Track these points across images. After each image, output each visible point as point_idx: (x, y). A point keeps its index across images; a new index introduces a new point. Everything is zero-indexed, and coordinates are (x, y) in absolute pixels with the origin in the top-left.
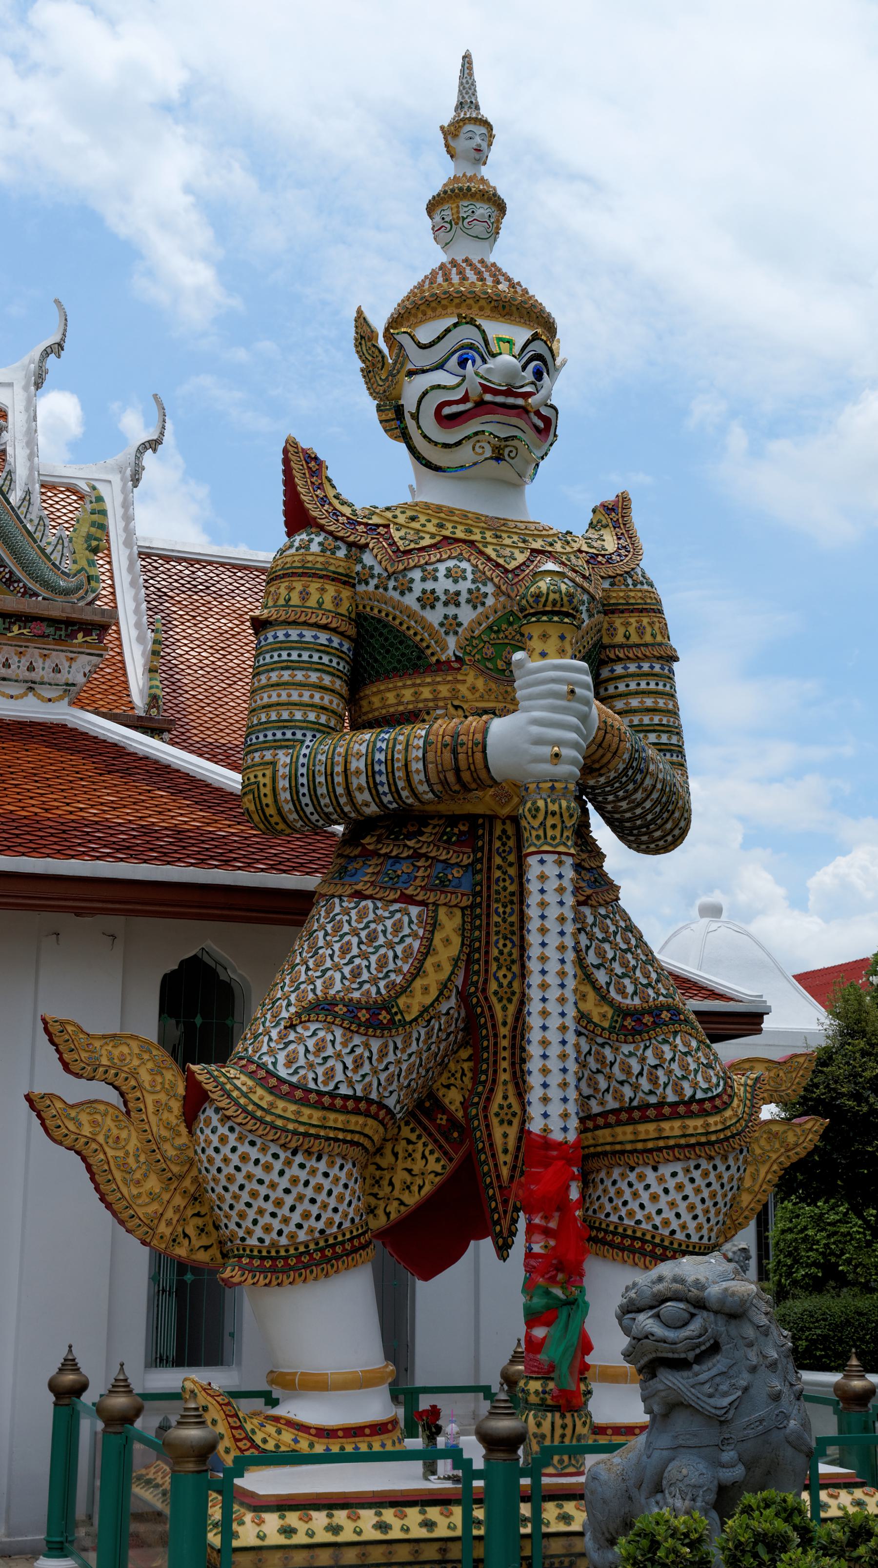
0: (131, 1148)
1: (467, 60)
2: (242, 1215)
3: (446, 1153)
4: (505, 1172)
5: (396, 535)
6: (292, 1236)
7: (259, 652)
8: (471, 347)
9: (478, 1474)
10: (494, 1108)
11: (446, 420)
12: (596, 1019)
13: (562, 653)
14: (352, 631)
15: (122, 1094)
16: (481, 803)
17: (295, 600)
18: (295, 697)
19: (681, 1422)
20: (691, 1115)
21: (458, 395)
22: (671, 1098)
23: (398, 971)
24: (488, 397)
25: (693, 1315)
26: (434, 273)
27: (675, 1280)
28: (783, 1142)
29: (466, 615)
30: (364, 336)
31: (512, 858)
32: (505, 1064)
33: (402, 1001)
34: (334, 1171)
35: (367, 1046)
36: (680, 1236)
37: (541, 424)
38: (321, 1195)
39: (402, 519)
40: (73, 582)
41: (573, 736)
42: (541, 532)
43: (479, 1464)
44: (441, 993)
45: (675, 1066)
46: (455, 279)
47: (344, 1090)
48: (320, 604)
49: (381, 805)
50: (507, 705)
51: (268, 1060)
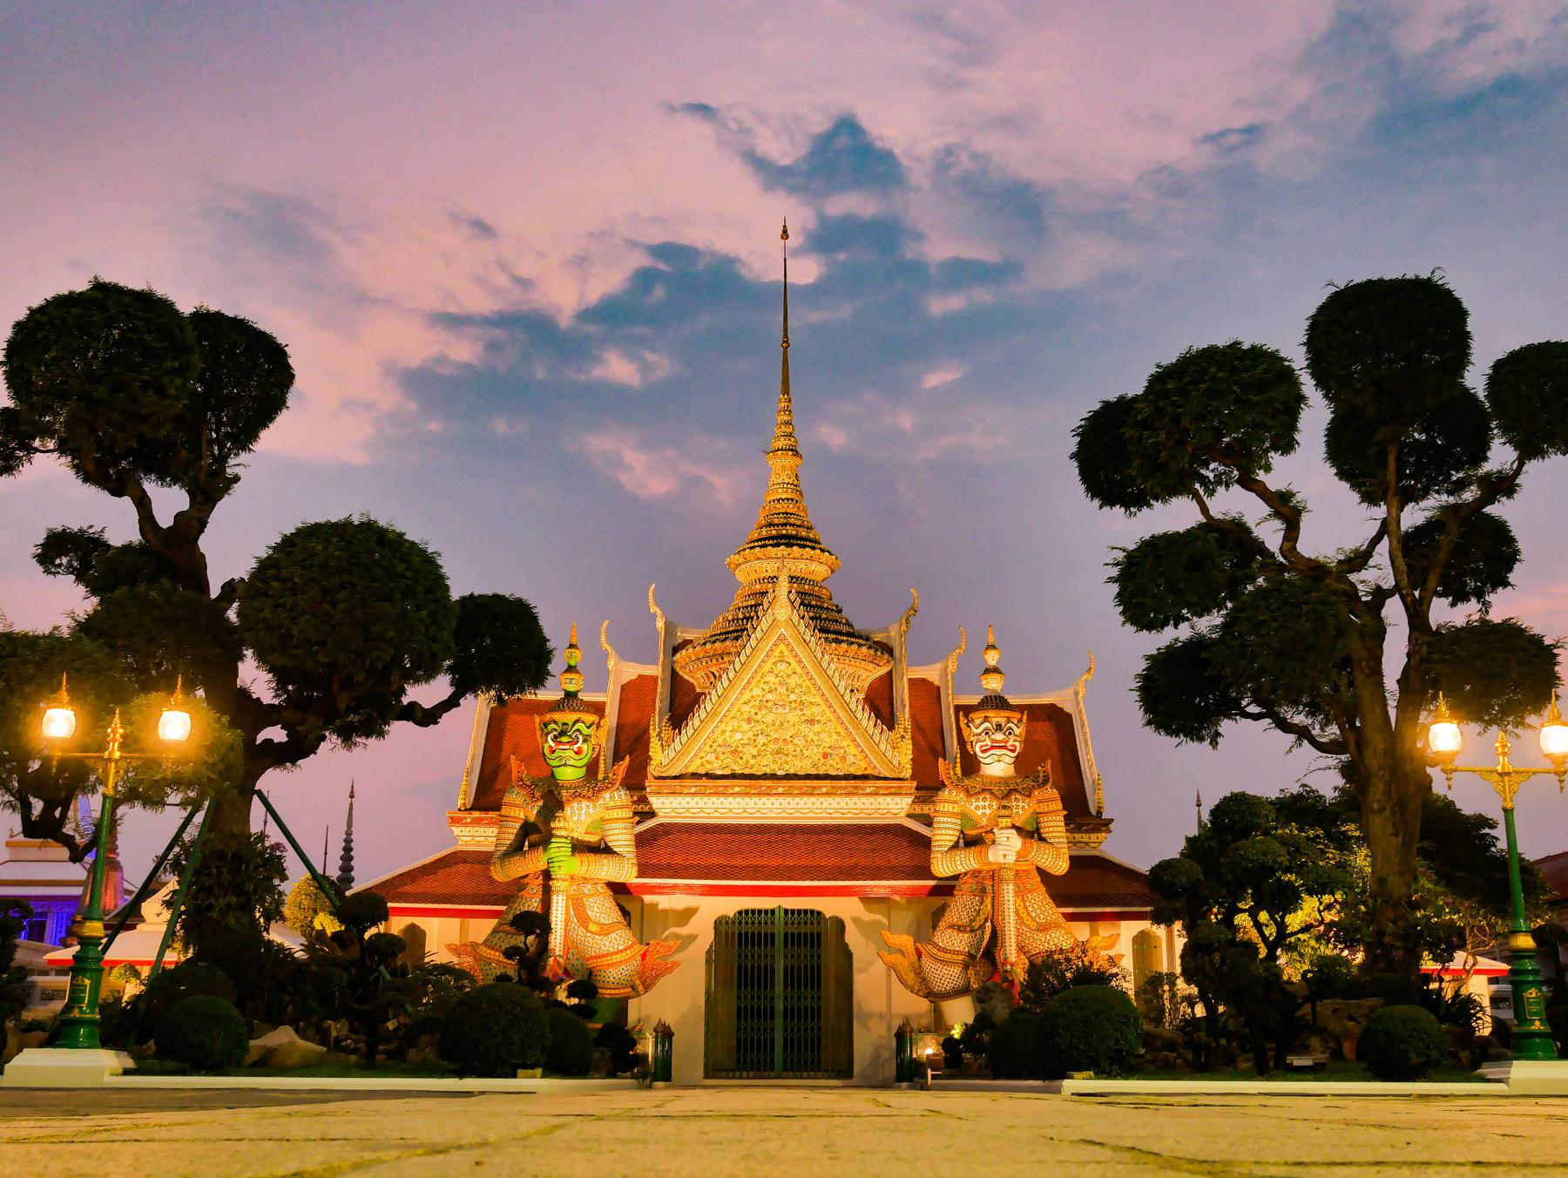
11: (984, 751)
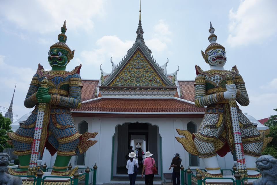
0: (187, 142)
1: (211, 23)
2: (201, 150)
3: (223, 142)
4: (232, 144)
5: (209, 73)
6: (207, 152)
7: (195, 88)
8: (215, 52)
9: (235, 181)
10: (229, 137)
11: (213, 60)
12: (241, 126)
13: (232, 84)
14: (205, 84)
15: (185, 137)
16: (223, 102)
17: (199, 82)
18: (200, 92)
19: (268, 177)
20: (255, 137)
21: (215, 57)
22: (252, 135)
23: (216, 122)
24: (218, 57)
25: (268, 163)
26: (210, 45)
27: (264, 158)
28: (267, 140)
29: (219, 81)
30: (203, 53)
31: (228, 108)
32: (230, 132)
33: (217, 125)
34: (211, 145)
35: (213, 130)
36: (256, 152)
37: (225, 59)
38: (209, 148)
39: (210, 72)
40: (172, 84)
41: (235, 93)
42: (226, 71)
43: (235, 180)
44: (221, 124)
45: (252, 131)
46: (212, 45)
47: (211, 135)
48: (201, 82)
49: (211, 103)
50: (226, 90)
51: (202, 132)
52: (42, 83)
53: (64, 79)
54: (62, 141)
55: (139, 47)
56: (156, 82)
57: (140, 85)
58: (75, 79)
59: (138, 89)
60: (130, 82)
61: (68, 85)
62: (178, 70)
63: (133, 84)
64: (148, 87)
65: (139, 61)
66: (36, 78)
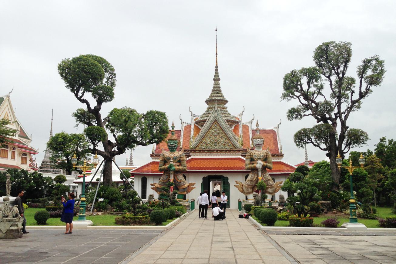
1: (257, 120)
29: (256, 158)
38: (250, 190)
50: (257, 164)
52: (170, 162)
53: (178, 157)
54: (181, 188)
55: (216, 119)
56: (228, 146)
57: (217, 148)
58: (183, 156)
59: (216, 151)
60: (210, 146)
61: (180, 160)
62: (253, 119)
63: (212, 147)
64: (223, 150)
65: (216, 130)
66: (163, 156)
